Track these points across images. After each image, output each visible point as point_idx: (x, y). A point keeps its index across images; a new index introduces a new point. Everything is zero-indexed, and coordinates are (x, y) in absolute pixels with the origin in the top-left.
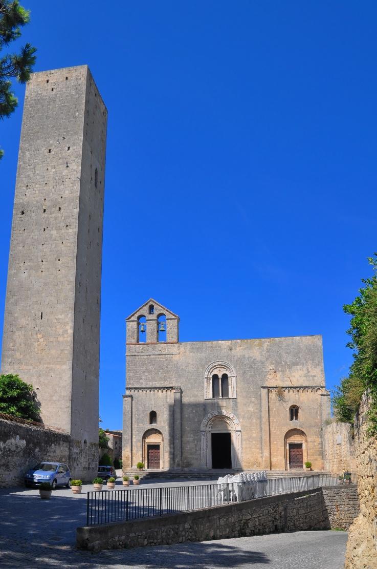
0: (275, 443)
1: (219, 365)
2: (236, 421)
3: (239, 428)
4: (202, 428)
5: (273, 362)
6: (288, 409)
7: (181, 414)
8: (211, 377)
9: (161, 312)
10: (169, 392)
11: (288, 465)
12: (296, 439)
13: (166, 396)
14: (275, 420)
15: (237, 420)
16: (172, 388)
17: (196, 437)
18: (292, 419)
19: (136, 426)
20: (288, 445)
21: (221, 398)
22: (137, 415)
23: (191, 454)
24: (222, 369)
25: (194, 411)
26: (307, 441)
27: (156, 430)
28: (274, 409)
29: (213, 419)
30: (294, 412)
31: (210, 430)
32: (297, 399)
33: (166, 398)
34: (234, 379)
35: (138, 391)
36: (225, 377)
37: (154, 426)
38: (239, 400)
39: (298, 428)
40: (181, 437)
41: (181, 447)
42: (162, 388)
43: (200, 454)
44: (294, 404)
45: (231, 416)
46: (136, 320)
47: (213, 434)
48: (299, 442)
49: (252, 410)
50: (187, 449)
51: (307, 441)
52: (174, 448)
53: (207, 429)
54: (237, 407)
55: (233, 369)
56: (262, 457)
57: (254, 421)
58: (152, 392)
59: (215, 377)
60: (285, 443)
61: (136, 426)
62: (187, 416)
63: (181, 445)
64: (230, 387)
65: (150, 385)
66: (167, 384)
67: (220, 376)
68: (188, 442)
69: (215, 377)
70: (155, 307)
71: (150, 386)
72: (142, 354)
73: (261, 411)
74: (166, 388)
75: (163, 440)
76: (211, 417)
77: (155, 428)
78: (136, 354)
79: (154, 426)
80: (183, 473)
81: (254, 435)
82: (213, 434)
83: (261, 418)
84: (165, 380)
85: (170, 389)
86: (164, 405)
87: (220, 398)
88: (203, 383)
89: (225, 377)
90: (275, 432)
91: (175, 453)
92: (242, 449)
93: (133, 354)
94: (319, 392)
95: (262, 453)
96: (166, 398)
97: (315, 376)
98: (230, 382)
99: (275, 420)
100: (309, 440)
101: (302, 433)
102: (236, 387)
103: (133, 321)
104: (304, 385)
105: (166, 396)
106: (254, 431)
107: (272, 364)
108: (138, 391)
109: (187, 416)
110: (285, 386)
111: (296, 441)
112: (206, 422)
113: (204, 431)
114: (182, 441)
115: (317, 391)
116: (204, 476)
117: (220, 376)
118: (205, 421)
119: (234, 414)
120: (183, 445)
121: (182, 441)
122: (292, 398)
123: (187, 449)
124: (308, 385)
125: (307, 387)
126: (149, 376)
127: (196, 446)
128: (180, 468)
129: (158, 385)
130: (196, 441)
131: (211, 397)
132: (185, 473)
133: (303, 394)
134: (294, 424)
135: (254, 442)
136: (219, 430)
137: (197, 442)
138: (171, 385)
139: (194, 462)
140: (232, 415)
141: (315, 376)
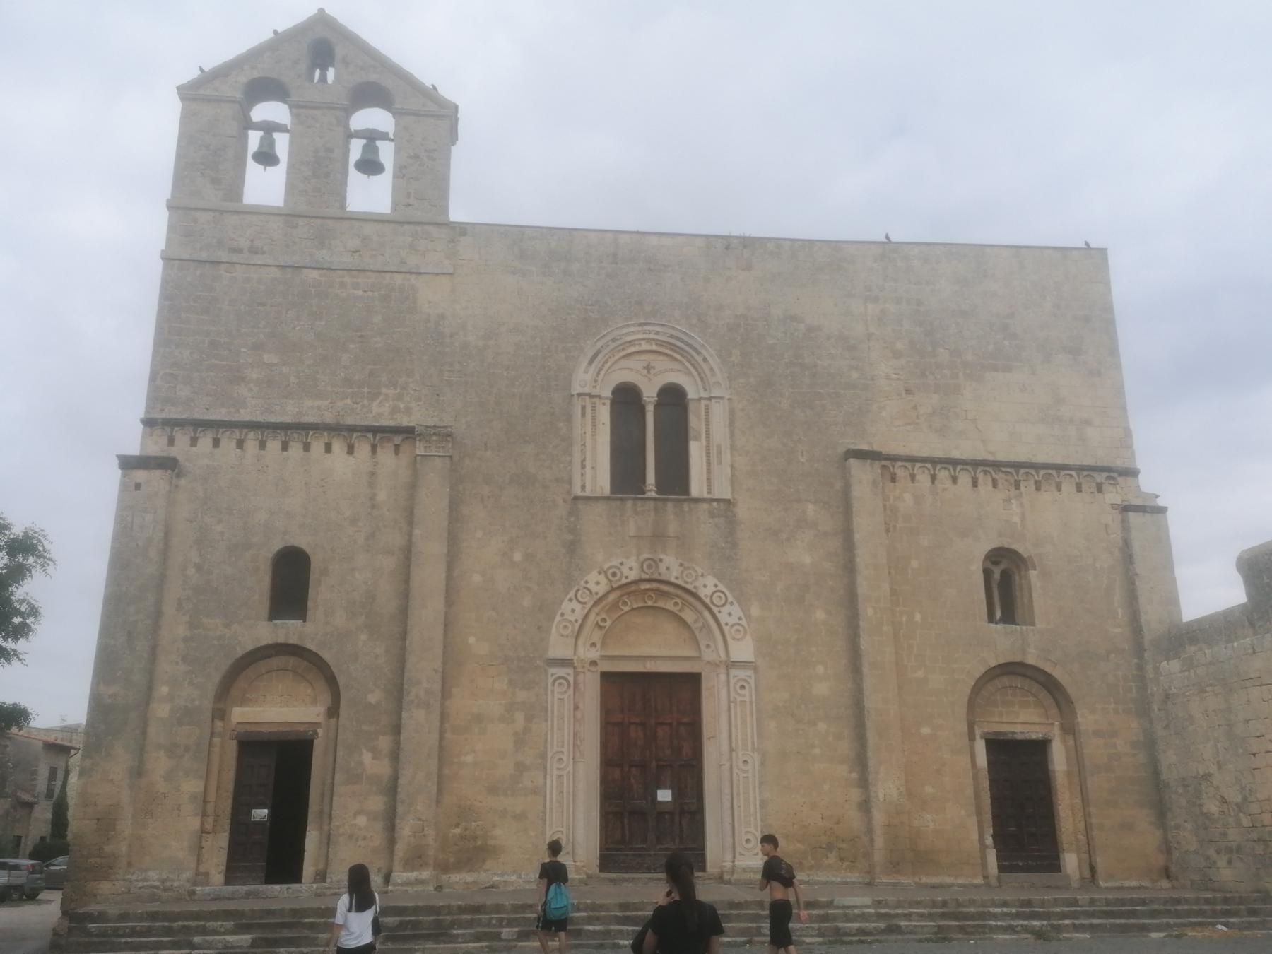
0: (926, 731)
1: (649, 341)
2: (730, 614)
3: (743, 650)
4: (559, 649)
5: (899, 346)
6: (977, 568)
7: (450, 567)
8: (607, 393)
9: (373, 77)
10: (386, 457)
11: (992, 857)
12: (1023, 719)
13: (372, 474)
14: (918, 617)
15: (736, 610)
16: (408, 433)
17: (522, 696)
18: (991, 619)
19: (182, 631)
20: (980, 747)
21: (653, 494)
22: (199, 568)
23: (493, 790)
24: (660, 363)
25: (518, 557)
26: (1070, 729)
27: (296, 651)
28: (914, 564)
29: (612, 597)
30: (1005, 581)
31: (594, 654)
32: (1016, 519)
33: (371, 485)
34: (719, 414)
35: (216, 443)
36: (673, 398)
37: (289, 631)
38: (742, 512)
39: (1031, 660)
40: (445, 694)
41: (441, 747)
42: (352, 429)
43: (537, 791)
44: (1006, 543)
45: (707, 586)
46: (238, 95)
47: (609, 679)
48: (1036, 734)
49: (808, 560)
50: (469, 759)
51: (1070, 729)
52: (395, 756)
53: (581, 651)
54: (734, 545)
55: (714, 362)
56: (865, 806)
57: (820, 615)
58: (295, 450)
59: (626, 398)
60: (972, 738)
61: (182, 631)
62: (477, 578)
63: (442, 738)
64: (696, 450)
65: (288, 412)
66: (381, 412)
67: (650, 394)
68: (478, 718)
69: (626, 398)
70: (339, 52)
71: (287, 419)
72: (258, 259)
73: (850, 568)
74: (375, 430)
75: (333, 712)
76: (602, 588)
77: (293, 640)
78: (223, 255)
79: (289, 631)
80: (462, 910)
81: (821, 689)
82: (609, 679)
83: (851, 599)
84: (373, 396)
85: (397, 439)
86: (354, 521)
87: (649, 494)
88: (569, 418)
89: (673, 398)
90: (920, 674)
91: (402, 781)
92: (762, 764)
93: (204, 255)
94: (1112, 496)
95: (864, 782)
96: (371, 485)
97: (1088, 422)
98: (693, 422)
99: (918, 617)
100: (1086, 719)
101: (1050, 685)
102: (733, 447)
103: (218, 101)
104: (1040, 458)
105: (372, 474)
106: (820, 669)
107: (897, 355)
108: (216, 443)
109: (477, 578)
110: (956, 454)
111: (1018, 729)
112: (580, 611)
113: (563, 663)
114: (444, 717)
115: (1100, 488)
116: (590, 920)
117: (650, 394)
118: (572, 610)
119: (721, 577)
120: (448, 735)
121: (444, 717)
122: (996, 516)
123: (469, 759)
124: (1059, 461)
125: (1060, 467)
126: (285, 370)
127: (520, 741)
128: (425, 874)
129: (329, 418)
130: (520, 717)
131: (607, 490)
132: (478, 909)
133: (1047, 496)
134: (1003, 643)
135: (822, 726)
136: (656, 650)
137: (529, 719)
138: (405, 421)
139: (504, 834)
140: (711, 581)
141: (1088, 422)
